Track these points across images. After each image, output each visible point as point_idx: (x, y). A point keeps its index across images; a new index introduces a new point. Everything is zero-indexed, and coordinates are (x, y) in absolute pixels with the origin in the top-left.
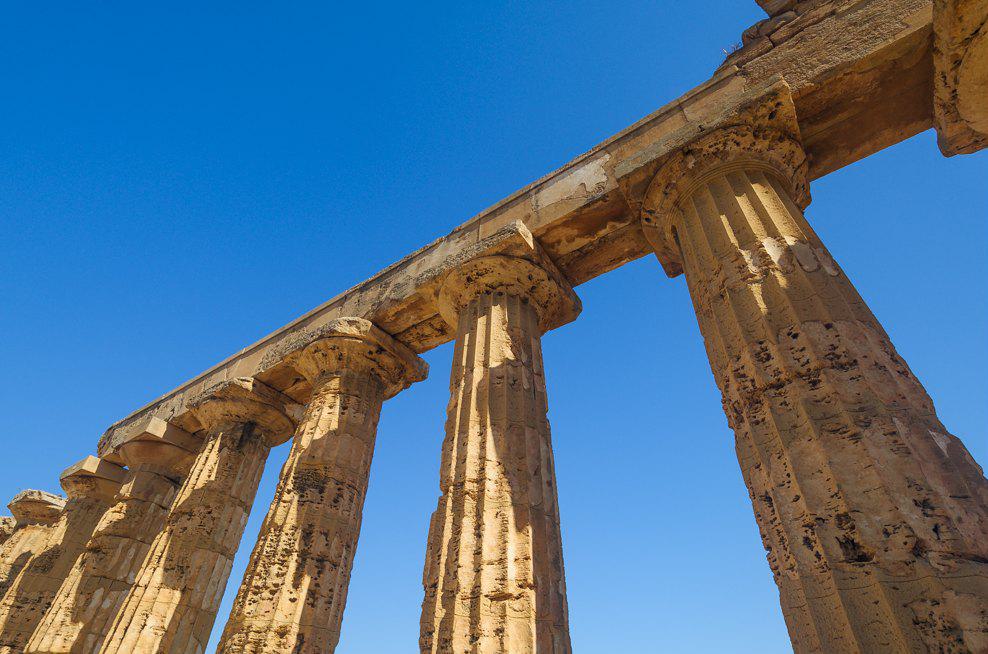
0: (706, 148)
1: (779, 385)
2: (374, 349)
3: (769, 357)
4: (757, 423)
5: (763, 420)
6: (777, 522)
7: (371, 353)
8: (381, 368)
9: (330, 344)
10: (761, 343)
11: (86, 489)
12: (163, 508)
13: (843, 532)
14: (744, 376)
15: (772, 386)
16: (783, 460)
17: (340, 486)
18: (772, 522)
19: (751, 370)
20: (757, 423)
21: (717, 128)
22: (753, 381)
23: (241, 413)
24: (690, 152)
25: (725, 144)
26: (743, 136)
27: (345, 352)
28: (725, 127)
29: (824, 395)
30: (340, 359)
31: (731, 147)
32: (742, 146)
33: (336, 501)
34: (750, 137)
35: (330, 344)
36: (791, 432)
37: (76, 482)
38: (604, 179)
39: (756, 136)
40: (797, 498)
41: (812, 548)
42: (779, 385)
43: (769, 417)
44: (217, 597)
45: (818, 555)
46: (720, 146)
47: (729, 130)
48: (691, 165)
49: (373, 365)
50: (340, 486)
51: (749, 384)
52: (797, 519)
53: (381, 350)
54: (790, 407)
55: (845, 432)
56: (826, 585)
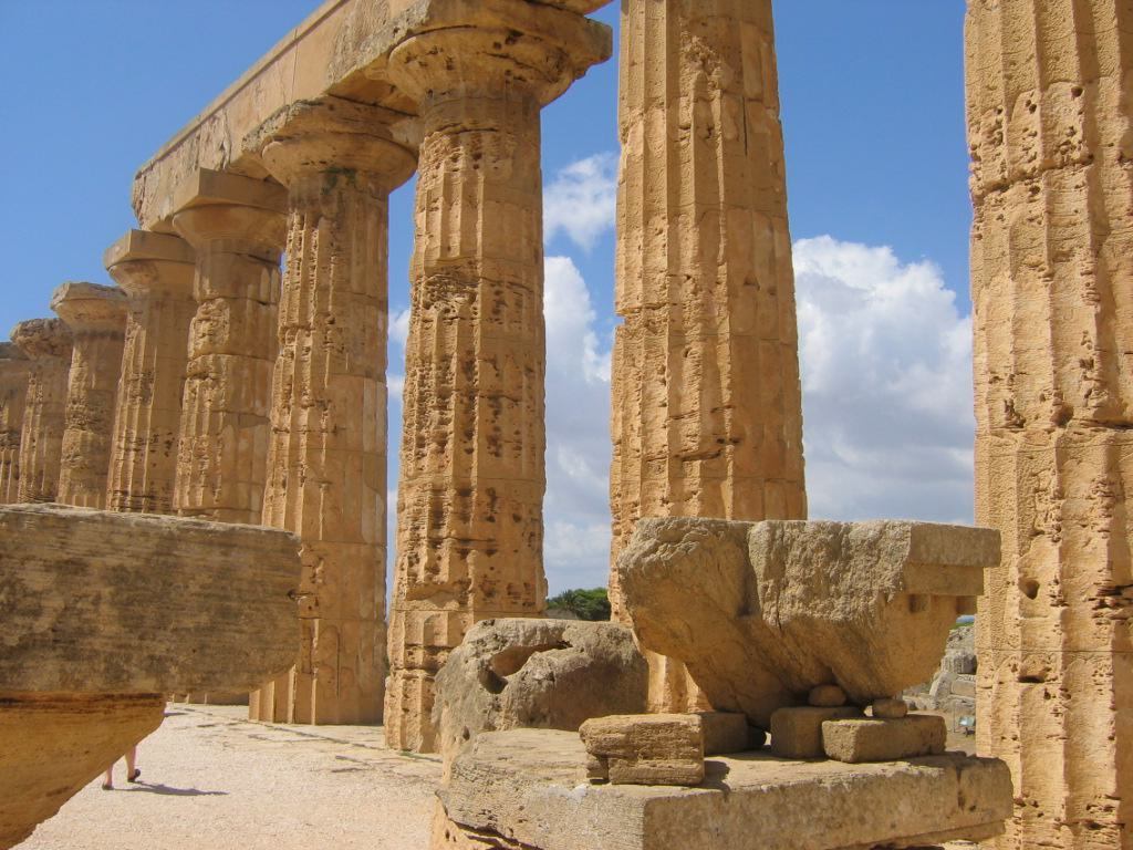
2: (501, 39)
7: (497, 45)
8: (520, 65)
9: (428, 44)
11: (146, 280)
12: (264, 304)
17: (497, 288)
23: (327, 158)
27: (455, 54)
30: (449, 68)
33: (496, 312)
35: (428, 44)
37: (130, 271)
44: (380, 432)
49: (507, 65)
50: (497, 288)
53: (513, 36)
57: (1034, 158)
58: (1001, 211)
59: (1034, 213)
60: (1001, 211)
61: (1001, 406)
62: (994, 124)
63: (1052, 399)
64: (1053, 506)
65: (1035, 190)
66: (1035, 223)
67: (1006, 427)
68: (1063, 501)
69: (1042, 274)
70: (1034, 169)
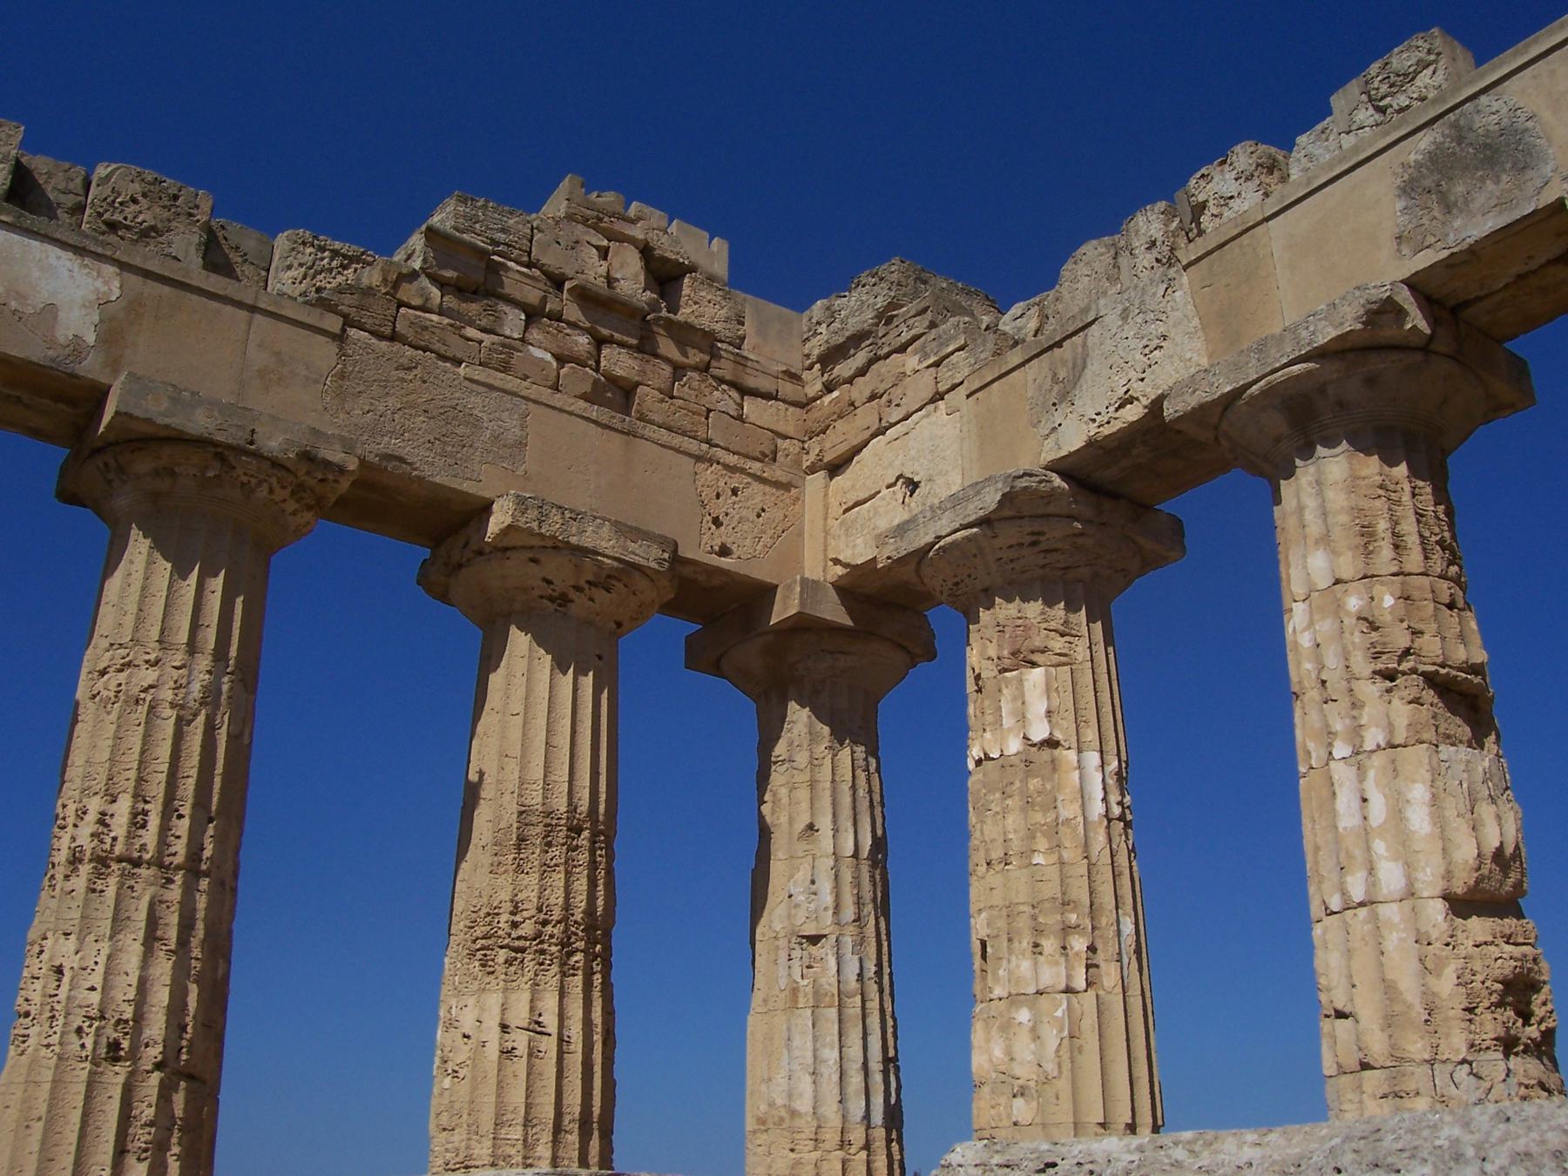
0: (240, 471)
1: (137, 863)
3: (144, 826)
4: (94, 891)
5: (102, 891)
6: (56, 999)
10: (146, 802)
13: (116, 1035)
14: (107, 826)
15: (130, 861)
16: (99, 945)
18: (51, 996)
19: (120, 825)
20: (94, 891)
21: (267, 458)
22: (115, 839)
24: (221, 457)
25: (260, 483)
26: (284, 488)
28: (276, 464)
29: (169, 899)
31: (263, 493)
32: (272, 497)
34: (286, 493)
36: (119, 921)
38: (91, 338)
39: (293, 493)
40: (93, 989)
41: (81, 1038)
42: (137, 863)
43: (111, 892)
45: (83, 1046)
46: (253, 481)
47: (275, 471)
48: (210, 474)
51: (108, 840)
52: (80, 1007)
54: (134, 894)
55: (166, 945)
56: (75, 1073)
57: (175, 854)
58: (132, 882)
59: (165, 898)
60: (132, 882)
61: (104, 1041)
62: (140, 810)
63: (160, 1048)
64: (142, 1132)
65: (169, 881)
66: (164, 906)
67: (105, 1059)
68: (153, 1130)
69: (164, 948)
70: (171, 863)
